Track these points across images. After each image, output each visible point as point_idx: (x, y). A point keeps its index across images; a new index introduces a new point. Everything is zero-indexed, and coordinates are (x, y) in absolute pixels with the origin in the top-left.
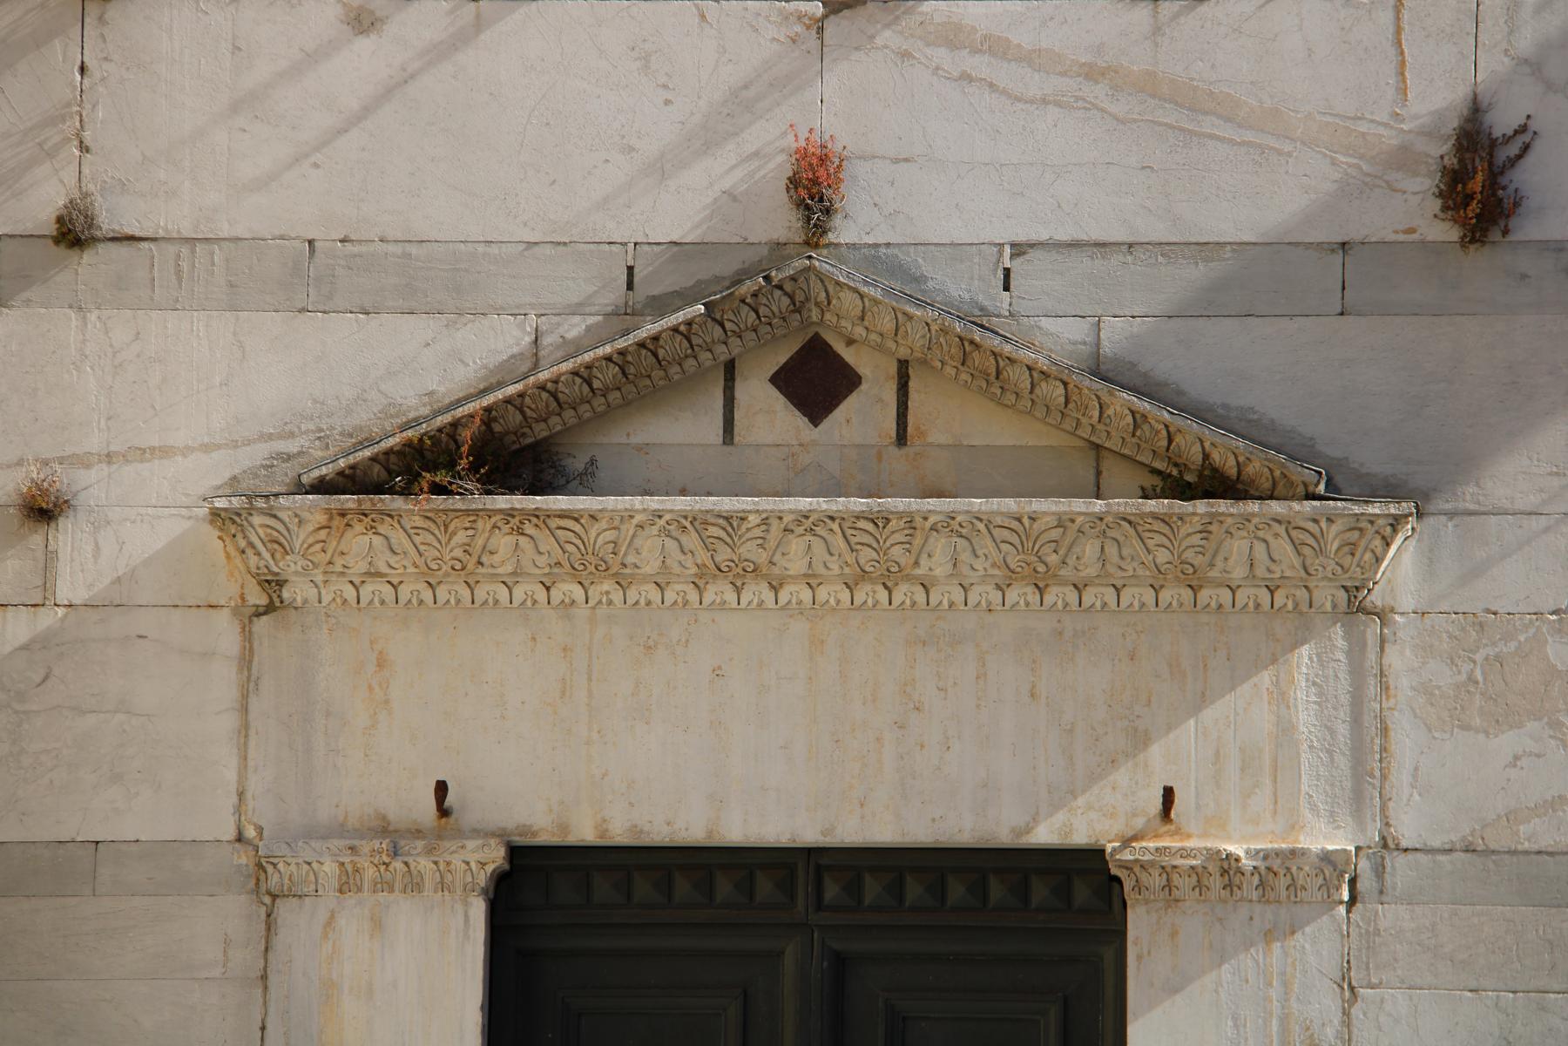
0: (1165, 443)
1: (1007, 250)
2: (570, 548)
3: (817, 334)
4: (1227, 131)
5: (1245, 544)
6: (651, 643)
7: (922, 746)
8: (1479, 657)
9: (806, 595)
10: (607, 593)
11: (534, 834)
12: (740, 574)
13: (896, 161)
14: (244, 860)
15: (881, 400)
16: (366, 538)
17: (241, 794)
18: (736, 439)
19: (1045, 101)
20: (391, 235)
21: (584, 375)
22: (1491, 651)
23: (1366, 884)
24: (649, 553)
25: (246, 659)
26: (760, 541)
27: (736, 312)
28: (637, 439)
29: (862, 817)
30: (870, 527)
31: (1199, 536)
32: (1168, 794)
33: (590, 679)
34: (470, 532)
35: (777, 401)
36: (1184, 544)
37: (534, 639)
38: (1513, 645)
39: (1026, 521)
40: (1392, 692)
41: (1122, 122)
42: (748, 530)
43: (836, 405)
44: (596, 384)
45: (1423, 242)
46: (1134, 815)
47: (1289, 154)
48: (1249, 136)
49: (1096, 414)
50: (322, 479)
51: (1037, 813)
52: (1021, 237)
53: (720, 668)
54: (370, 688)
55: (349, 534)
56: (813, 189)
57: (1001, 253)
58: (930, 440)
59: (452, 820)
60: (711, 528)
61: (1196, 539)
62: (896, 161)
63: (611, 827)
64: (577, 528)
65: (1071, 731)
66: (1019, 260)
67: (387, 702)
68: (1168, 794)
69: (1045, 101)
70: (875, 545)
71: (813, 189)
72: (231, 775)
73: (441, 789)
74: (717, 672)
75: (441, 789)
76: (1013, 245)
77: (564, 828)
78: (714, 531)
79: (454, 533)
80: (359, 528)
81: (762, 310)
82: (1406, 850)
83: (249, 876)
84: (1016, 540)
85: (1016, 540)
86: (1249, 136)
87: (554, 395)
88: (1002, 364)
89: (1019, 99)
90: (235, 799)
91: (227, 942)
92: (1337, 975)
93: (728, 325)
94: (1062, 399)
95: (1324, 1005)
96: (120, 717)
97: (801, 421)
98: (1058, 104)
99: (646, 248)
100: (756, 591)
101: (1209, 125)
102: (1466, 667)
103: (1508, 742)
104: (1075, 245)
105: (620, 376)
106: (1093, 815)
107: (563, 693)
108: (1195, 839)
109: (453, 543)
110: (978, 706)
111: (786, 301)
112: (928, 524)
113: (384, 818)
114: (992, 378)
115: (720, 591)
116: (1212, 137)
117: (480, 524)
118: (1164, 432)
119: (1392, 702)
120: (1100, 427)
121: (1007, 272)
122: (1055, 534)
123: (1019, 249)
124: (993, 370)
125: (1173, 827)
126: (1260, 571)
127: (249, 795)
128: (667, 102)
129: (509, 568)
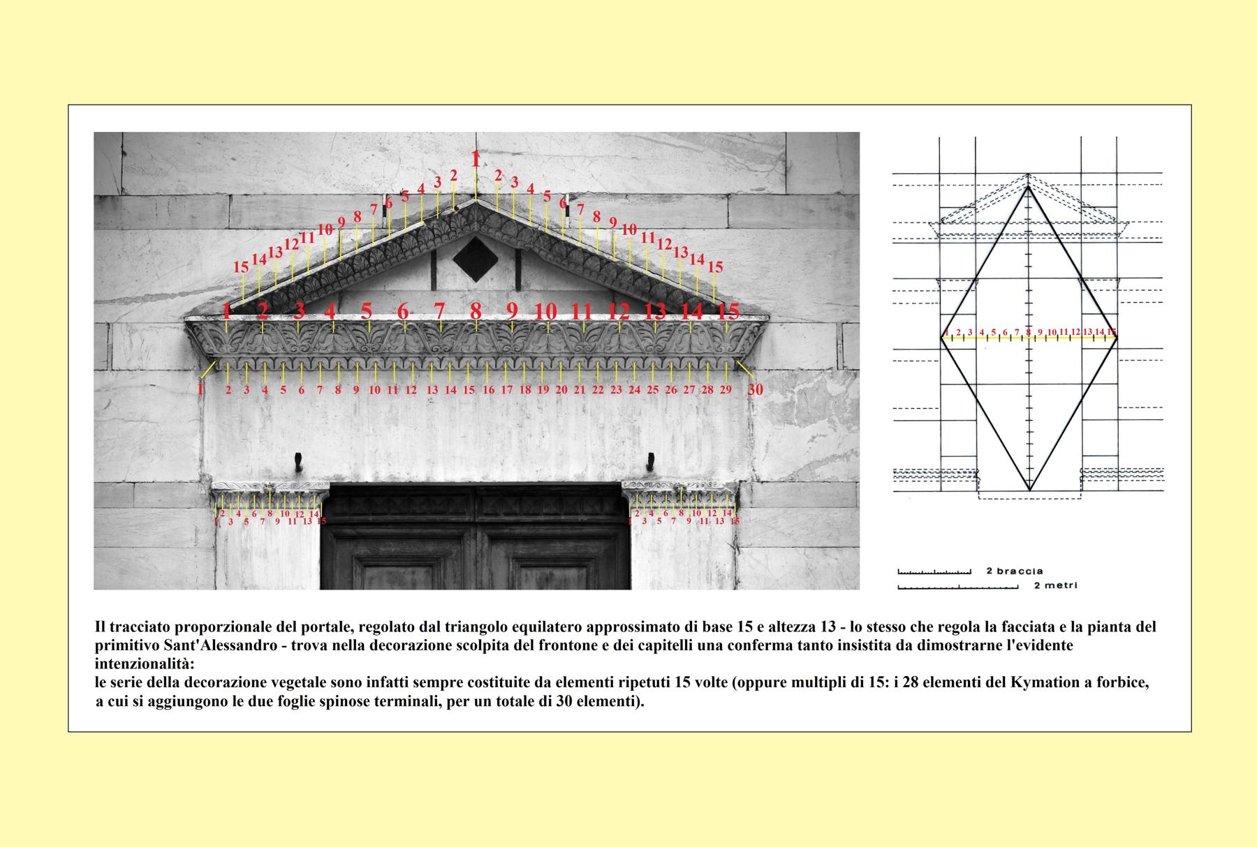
5: (687, 337)
8: (796, 390)
9: (474, 362)
12: (442, 353)
13: (514, 154)
20: (268, 191)
21: (367, 255)
22: (802, 387)
23: (744, 498)
28: (388, 289)
30: (507, 328)
32: (651, 456)
38: (811, 385)
44: (372, 260)
50: (240, 307)
62: (514, 154)
68: (651, 456)
72: (197, 452)
76: (571, 194)
77: (357, 476)
91: (197, 531)
95: (725, 554)
96: (144, 424)
97: (470, 279)
100: (449, 361)
102: (790, 395)
103: (810, 430)
121: (567, 208)
123: (573, 197)
126: (694, 350)
129: (330, 350)
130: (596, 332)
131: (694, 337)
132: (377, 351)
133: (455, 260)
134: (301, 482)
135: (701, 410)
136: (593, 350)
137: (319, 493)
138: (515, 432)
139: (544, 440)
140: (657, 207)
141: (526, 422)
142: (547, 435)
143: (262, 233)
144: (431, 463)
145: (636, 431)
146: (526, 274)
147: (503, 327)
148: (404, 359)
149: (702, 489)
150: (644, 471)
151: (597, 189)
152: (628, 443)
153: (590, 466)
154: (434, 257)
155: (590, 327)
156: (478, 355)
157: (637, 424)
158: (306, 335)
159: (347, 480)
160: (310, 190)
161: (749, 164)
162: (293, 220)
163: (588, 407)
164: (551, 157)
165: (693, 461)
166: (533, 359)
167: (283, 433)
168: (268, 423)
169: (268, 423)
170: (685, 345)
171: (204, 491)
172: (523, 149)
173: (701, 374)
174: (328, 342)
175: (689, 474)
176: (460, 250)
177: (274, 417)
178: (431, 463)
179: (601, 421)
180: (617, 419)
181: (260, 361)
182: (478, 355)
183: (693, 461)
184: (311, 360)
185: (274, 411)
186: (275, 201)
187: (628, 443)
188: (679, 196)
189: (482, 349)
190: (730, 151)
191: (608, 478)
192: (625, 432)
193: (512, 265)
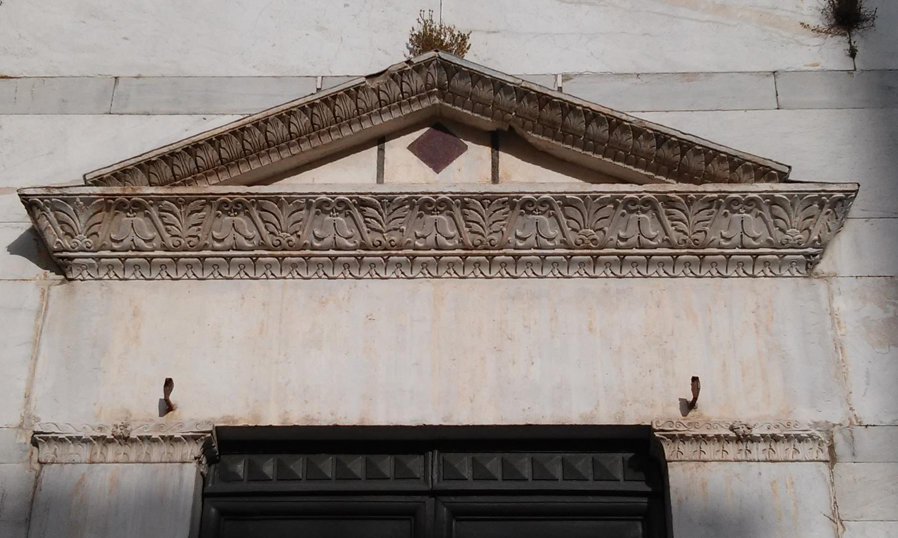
1: (560, 78)
6: (324, 300)
14: (23, 440)
15: (481, 158)
17: (27, 397)
18: (385, 181)
23: (841, 448)
25: (42, 312)
32: (695, 380)
35: (413, 159)
37: (243, 298)
40: (842, 325)
43: (452, 161)
44: (293, 129)
45: (822, 71)
52: (569, 71)
53: (371, 315)
58: (513, 180)
59: (176, 413)
62: (488, 32)
67: (137, 337)
68: (695, 380)
70: (483, 223)
74: (370, 318)
75: (169, 384)
82: (866, 426)
83: (26, 451)
86: (707, 17)
90: (22, 401)
92: (829, 512)
97: (429, 170)
104: (602, 75)
108: (715, 411)
113: (128, 412)
119: (843, 331)
125: (697, 413)
127: (33, 397)
132: (293, 243)
133: (412, 148)
137: (195, 438)
143: (154, 118)
149: (777, 432)
151: (597, 68)
159: (241, 424)
160: (221, 71)
161: (799, 38)
171: (26, 439)
191: (631, 419)
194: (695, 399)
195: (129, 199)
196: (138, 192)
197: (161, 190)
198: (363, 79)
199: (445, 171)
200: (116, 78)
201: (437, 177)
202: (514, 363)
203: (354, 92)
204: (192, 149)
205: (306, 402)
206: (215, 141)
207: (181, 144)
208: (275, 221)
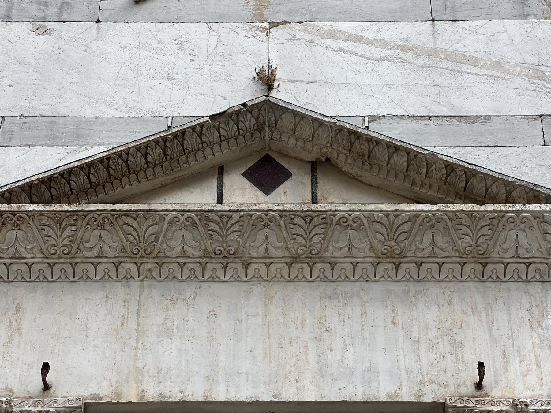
0: (463, 184)
1: (366, 119)
2: (131, 238)
3: (267, 156)
4: (475, 70)
5: (513, 233)
7: (331, 350)
10: (150, 270)
11: (100, 398)
12: (226, 257)
13: (308, 83)
16: (14, 232)
19: (381, 59)
20: (45, 113)
24: (175, 242)
26: (238, 233)
27: (227, 124)
29: (297, 388)
31: (488, 227)
32: (481, 365)
33: (138, 317)
34: (74, 228)
35: (247, 184)
36: (480, 233)
37: (108, 296)
39: (391, 218)
41: (422, 67)
42: (232, 225)
43: (278, 186)
44: (149, 159)
46: (459, 386)
47: (508, 79)
48: (486, 72)
49: (424, 171)
51: (401, 385)
52: (374, 113)
53: (213, 311)
54: (10, 322)
55: (4, 231)
56: (267, 80)
57: (364, 120)
59: (51, 391)
60: (211, 224)
61: (485, 230)
62: (308, 83)
63: (147, 394)
64: (135, 224)
65: (418, 342)
66: (373, 123)
67: (19, 329)
68: (481, 365)
69: (381, 59)
70: (304, 235)
71: (267, 80)
73: (46, 367)
75: (46, 367)
76: (369, 117)
77: (119, 395)
78: (212, 226)
79: (65, 229)
80: (9, 226)
81: (241, 125)
84: (384, 231)
85: (384, 231)
86: (486, 72)
87: (126, 162)
88: (372, 146)
89: (367, 58)
93: (222, 131)
94: (405, 164)
97: (260, 193)
98: (389, 61)
99: (179, 119)
100: (235, 266)
101: (465, 68)
104: (402, 117)
105: (162, 155)
106: (434, 386)
107: (123, 324)
109: (64, 236)
110: (363, 329)
111: (253, 121)
112: (335, 219)
114: (366, 158)
115: (214, 266)
116: (468, 73)
117: (79, 222)
118: (464, 177)
120: (426, 181)
122: (406, 227)
124: (366, 152)
125: (483, 393)
126: (521, 252)
128: (191, 60)
130: (406, 227)
131: (522, 235)
133: (245, 175)
134: (47, 400)
135: (535, 324)
136: (402, 255)
138: (311, 345)
139: (347, 355)
140: (465, 127)
141: (326, 335)
142: (351, 350)
143: (34, 150)
144: (211, 379)
145: (458, 345)
146: (321, 184)
147: (297, 220)
148: (182, 266)
150: (470, 389)
151: (397, 111)
152: (450, 359)
153: (405, 383)
154: (221, 172)
155: (399, 221)
156: (268, 260)
157: (458, 338)
158: (68, 231)
160: (90, 112)
162: (70, 139)
163: (399, 320)
164: (347, 85)
165: (532, 379)
166: (333, 265)
167: (32, 347)
168: (16, 337)
169: (16, 337)
170: (510, 244)
172: (318, 78)
173: (530, 286)
174: (94, 241)
175: (529, 393)
176: (249, 166)
177: (24, 331)
178: (211, 379)
179: (415, 334)
180: (434, 332)
181: (14, 268)
182: (268, 260)
183: (532, 379)
184: (74, 265)
185: (25, 324)
186: (52, 122)
187: (449, 358)
188: (488, 118)
189: (273, 252)
190: (540, 78)
192: (445, 346)
193: (307, 180)
194: (481, 380)
195: (14, 215)
196: (23, 209)
197: (41, 208)
198: (208, 119)
199: (273, 194)
200: (3, 117)
201: (267, 198)
202: (331, 350)
203: (199, 129)
204: (67, 174)
205: (160, 382)
206: (87, 168)
207: (58, 171)
208: (135, 233)
